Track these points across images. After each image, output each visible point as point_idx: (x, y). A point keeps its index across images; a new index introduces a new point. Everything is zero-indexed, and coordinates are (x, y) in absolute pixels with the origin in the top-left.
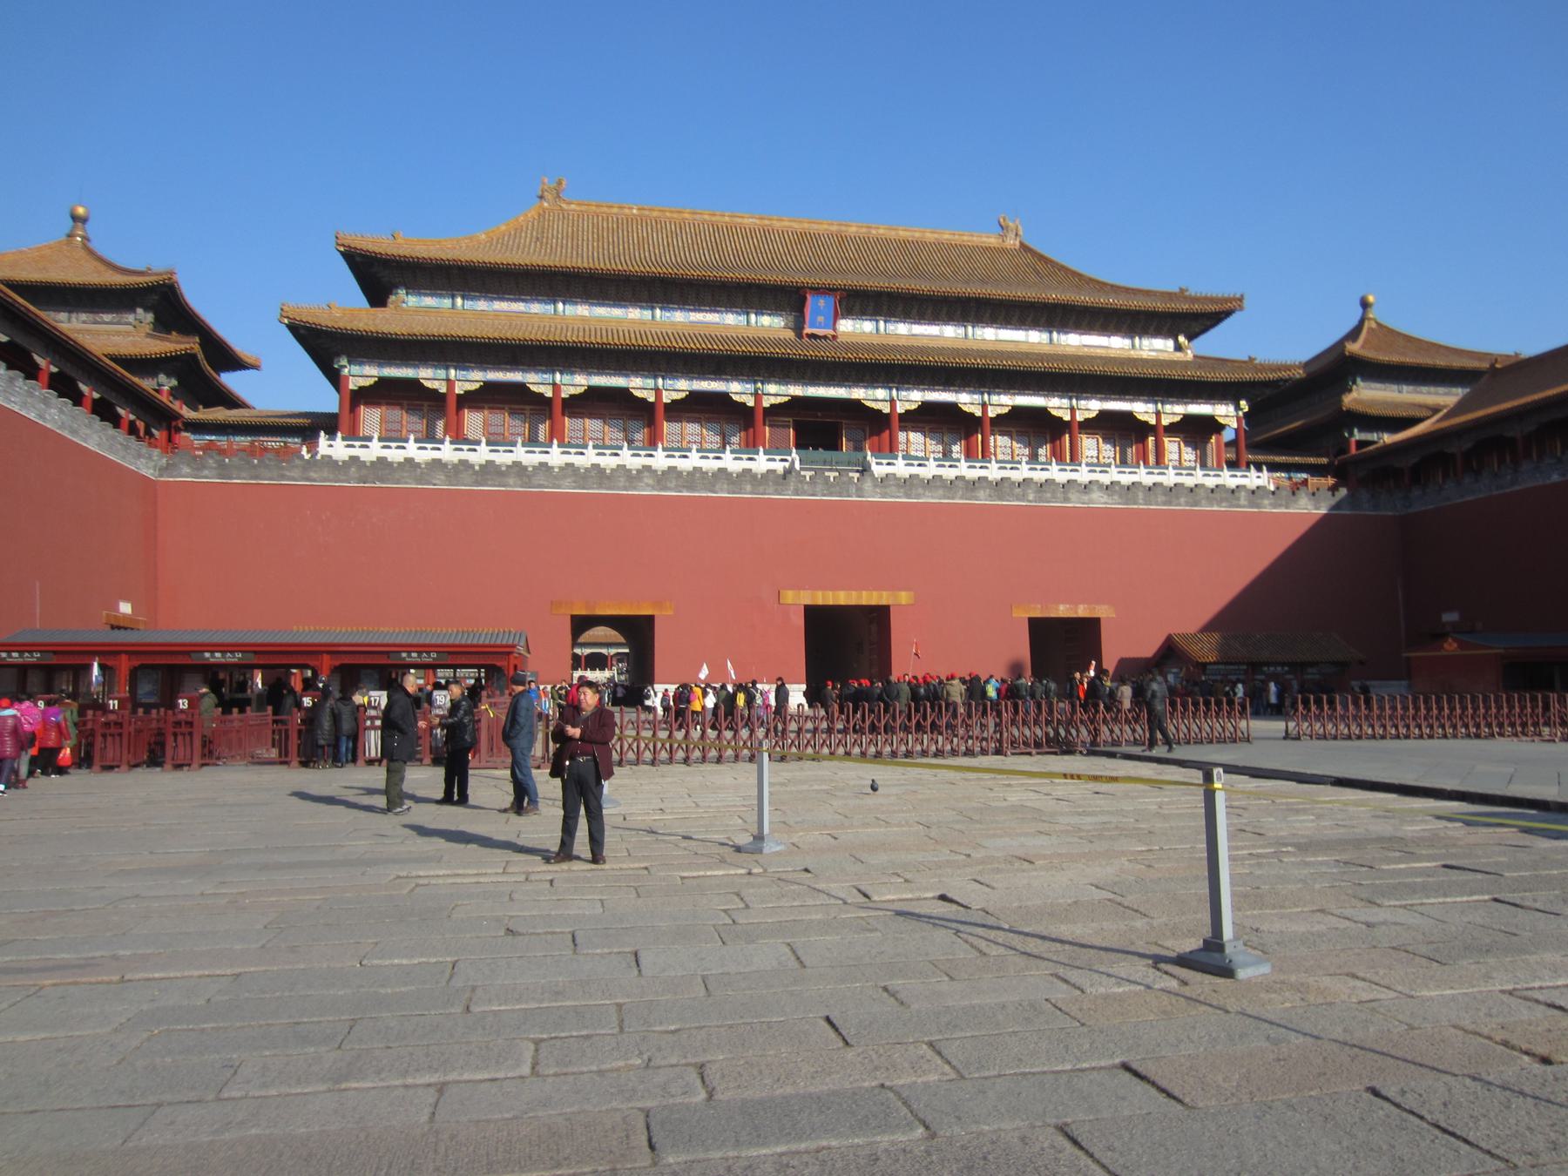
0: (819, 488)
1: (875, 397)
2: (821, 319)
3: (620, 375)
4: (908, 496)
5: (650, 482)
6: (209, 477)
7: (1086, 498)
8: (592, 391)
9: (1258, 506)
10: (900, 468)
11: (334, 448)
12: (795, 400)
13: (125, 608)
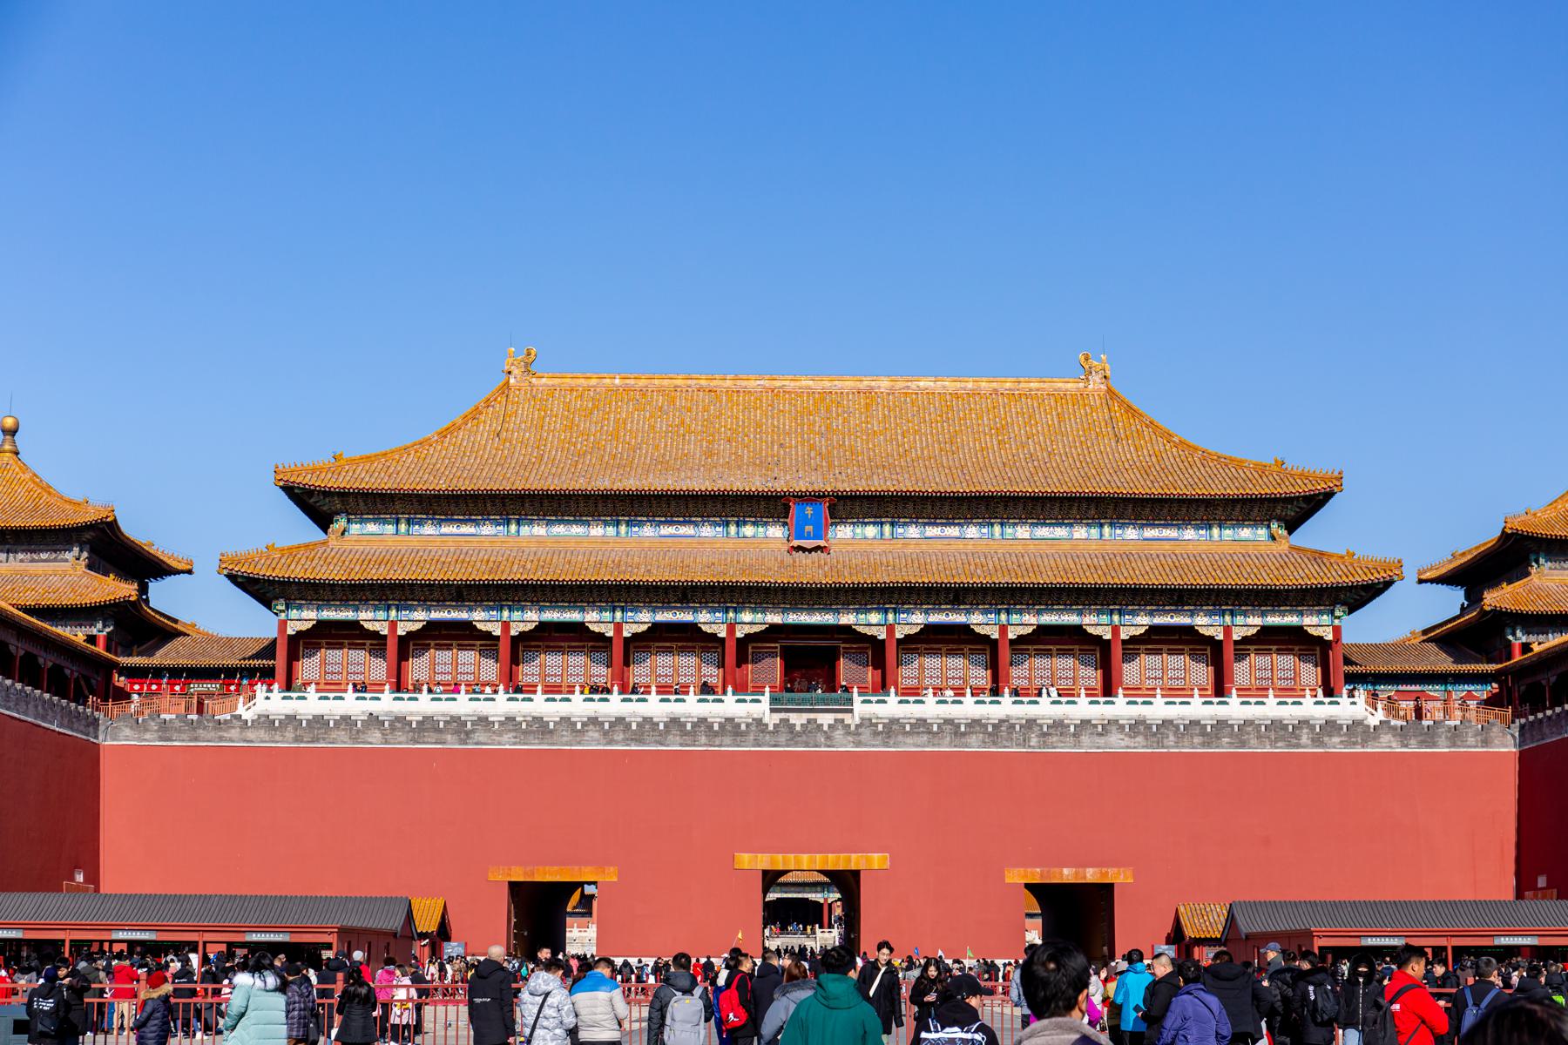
0: (782, 739)
1: (870, 622)
2: (809, 528)
3: (574, 608)
4: (886, 745)
5: (596, 735)
6: (151, 739)
7: (1101, 740)
8: (543, 626)
9: (1322, 744)
10: (891, 707)
11: (269, 702)
12: (773, 628)
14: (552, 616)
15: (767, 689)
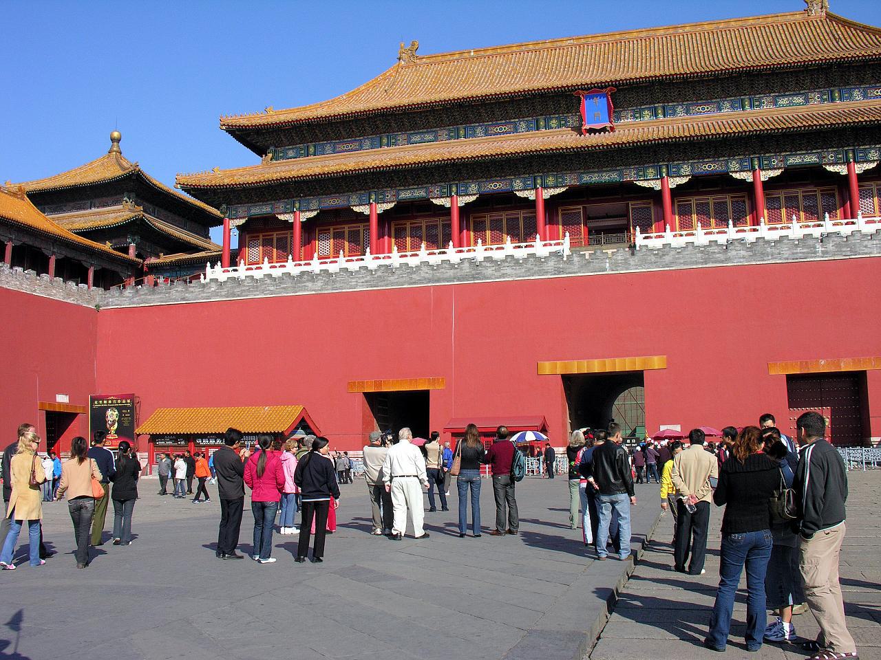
11: (216, 273)
13: (62, 399)
14: (405, 195)
15: (567, 234)
